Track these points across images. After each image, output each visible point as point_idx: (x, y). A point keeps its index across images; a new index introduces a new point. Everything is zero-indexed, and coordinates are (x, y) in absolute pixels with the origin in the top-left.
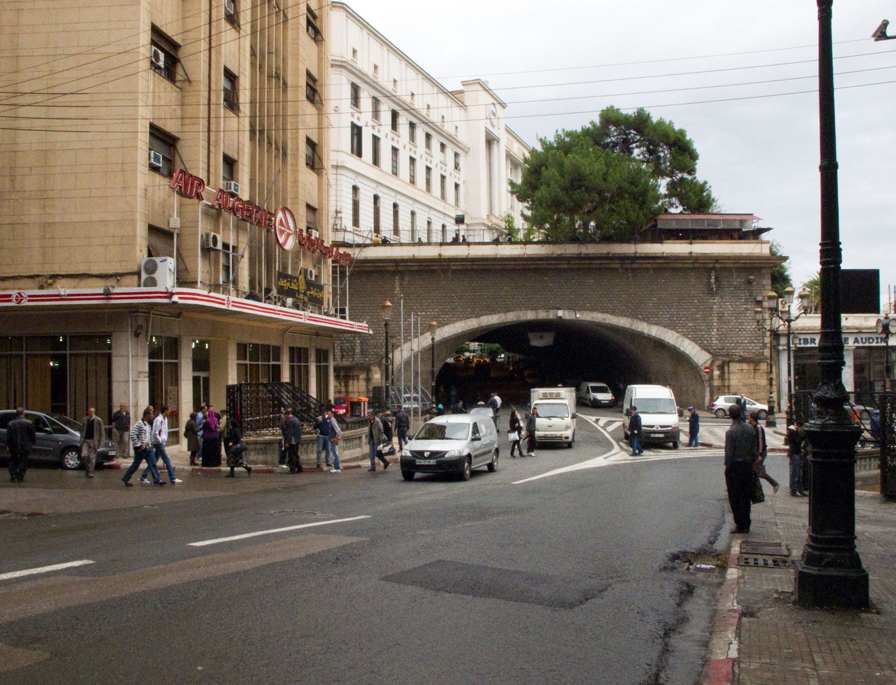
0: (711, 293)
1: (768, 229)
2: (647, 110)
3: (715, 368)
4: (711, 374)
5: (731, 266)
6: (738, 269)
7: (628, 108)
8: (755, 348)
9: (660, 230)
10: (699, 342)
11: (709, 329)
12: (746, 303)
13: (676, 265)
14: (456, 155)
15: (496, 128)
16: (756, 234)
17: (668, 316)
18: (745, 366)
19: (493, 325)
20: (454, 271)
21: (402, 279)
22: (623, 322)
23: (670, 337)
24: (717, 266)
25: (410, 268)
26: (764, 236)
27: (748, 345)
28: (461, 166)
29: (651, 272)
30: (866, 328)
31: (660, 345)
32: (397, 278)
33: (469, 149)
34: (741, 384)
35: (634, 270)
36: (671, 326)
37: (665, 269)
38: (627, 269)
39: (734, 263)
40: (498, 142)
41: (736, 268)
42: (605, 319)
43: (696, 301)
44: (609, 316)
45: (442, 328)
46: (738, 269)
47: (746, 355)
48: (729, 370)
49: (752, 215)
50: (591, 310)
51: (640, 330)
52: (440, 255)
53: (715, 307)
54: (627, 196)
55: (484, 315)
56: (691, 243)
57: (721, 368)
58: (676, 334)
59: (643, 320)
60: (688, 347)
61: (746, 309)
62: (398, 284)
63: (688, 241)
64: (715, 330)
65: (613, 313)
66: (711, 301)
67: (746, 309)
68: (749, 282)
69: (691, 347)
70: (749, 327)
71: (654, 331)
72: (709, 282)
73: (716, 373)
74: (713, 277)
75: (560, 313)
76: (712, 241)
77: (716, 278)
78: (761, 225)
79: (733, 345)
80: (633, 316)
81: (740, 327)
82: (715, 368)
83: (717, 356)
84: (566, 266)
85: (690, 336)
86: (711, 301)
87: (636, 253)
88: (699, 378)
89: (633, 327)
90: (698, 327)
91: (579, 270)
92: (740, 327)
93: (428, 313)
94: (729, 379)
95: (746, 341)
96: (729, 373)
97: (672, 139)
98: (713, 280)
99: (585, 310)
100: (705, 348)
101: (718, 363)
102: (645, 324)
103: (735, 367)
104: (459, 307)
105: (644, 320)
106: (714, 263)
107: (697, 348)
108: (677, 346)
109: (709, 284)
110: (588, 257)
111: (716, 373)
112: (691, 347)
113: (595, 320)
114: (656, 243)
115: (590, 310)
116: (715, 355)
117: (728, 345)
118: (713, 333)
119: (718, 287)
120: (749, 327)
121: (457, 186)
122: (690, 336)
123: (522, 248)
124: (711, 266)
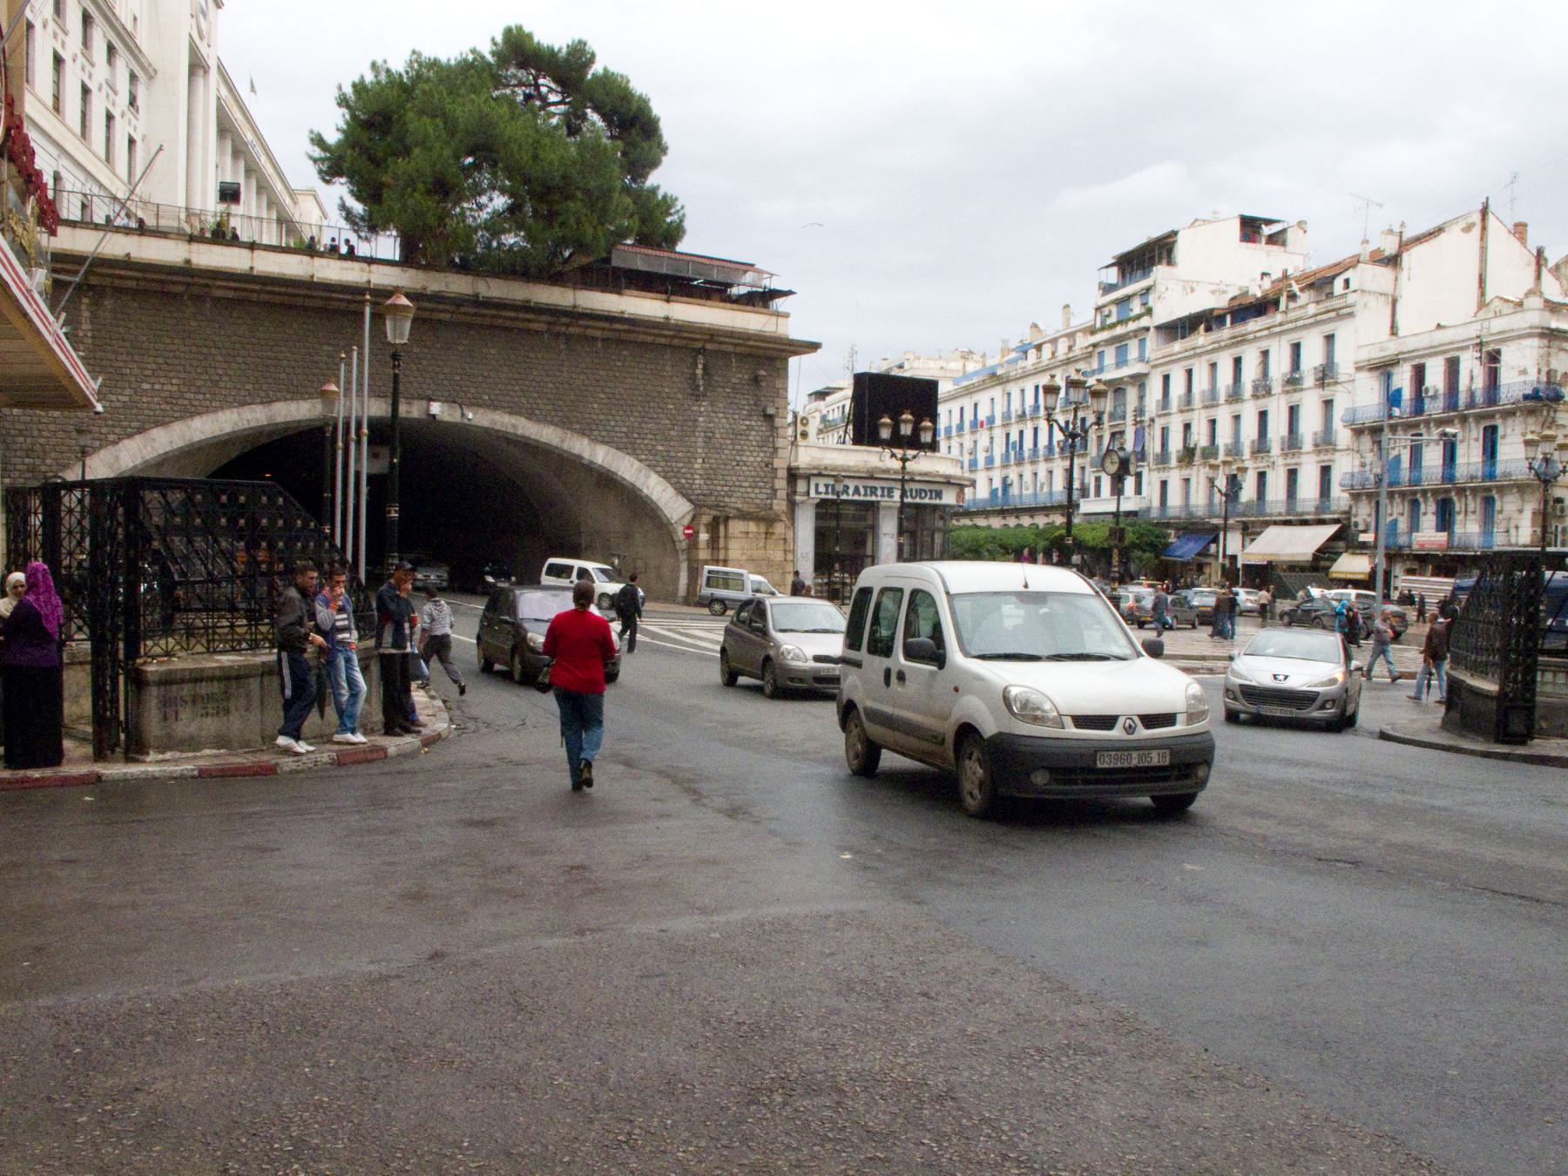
0: (697, 396)
1: (790, 293)
2: (593, 45)
3: (702, 528)
4: (692, 539)
5: (731, 349)
6: (742, 357)
7: (552, 35)
8: (759, 496)
9: (616, 270)
10: (675, 480)
11: (690, 461)
12: (749, 416)
13: (641, 338)
14: (133, 77)
15: (205, 42)
16: (762, 299)
17: (624, 429)
18: (752, 527)
19: (299, 421)
20: (216, 300)
21: (96, 304)
22: (546, 435)
23: (627, 468)
24: (709, 346)
25: (117, 282)
26: (779, 304)
27: (749, 490)
28: (140, 102)
29: (600, 345)
30: (920, 474)
31: (606, 481)
32: (85, 300)
33: (155, 70)
34: (744, 557)
35: (568, 337)
36: (628, 446)
37: (623, 342)
38: (558, 335)
39: (736, 345)
40: (206, 72)
41: (736, 354)
42: (514, 426)
43: (671, 407)
44: (523, 419)
45: (189, 422)
46: (742, 357)
47: (745, 508)
48: (726, 532)
49: (752, 265)
50: (493, 406)
51: (576, 451)
52: (188, 262)
53: (701, 419)
54: (579, 194)
55: (278, 400)
56: (668, 301)
57: (713, 527)
58: (637, 464)
59: (583, 433)
60: (656, 489)
61: (750, 428)
62: (87, 314)
63: (664, 296)
64: (700, 461)
65: (530, 415)
66: (695, 408)
67: (750, 428)
68: (756, 380)
69: (660, 488)
70: (751, 459)
71: (602, 455)
72: (694, 373)
73: (704, 537)
74: (700, 366)
75: (436, 408)
76: (699, 301)
77: (704, 369)
78: (775, 284)
79: (726, 489)
80: (565, 423)
81: (738, 458)
82: (702, 528)
83: (701, 507)
84: (447, 316)
85: (659, 469)
86: (695, 408)
87: (575, 307)
88: (669, 546)
89: (565, 446)
90: (672, 454)
91: (470, 326)
92: (738, 458)
93: (157, 387)
94: (726, 548)
95: (747, 484)
96: (726, 537)
97: (634, 106)
98: (699, 371)
99: (480, 406)
100: (683, 492)
101: (706, 519)
102: (586, 441)
103: (736, 527)
104: (225, 378)
105: (584, 434)
106: (706, 341)
107: (671, 491)
108: (638, 484)
109: (693, 377)
110: (489, 304)
111: (704, 537)
112: (660, 488)
113: (497, 427)
114: (611, 292)
115: (488, 407)
116: (698, 506)
117: (719, 488)
118: (696, 466)
119: (708, 386)
120: (751, 459)
121: (132, 142)
122: (659, 469)
123: (362, 270)
124: (699, 345)
